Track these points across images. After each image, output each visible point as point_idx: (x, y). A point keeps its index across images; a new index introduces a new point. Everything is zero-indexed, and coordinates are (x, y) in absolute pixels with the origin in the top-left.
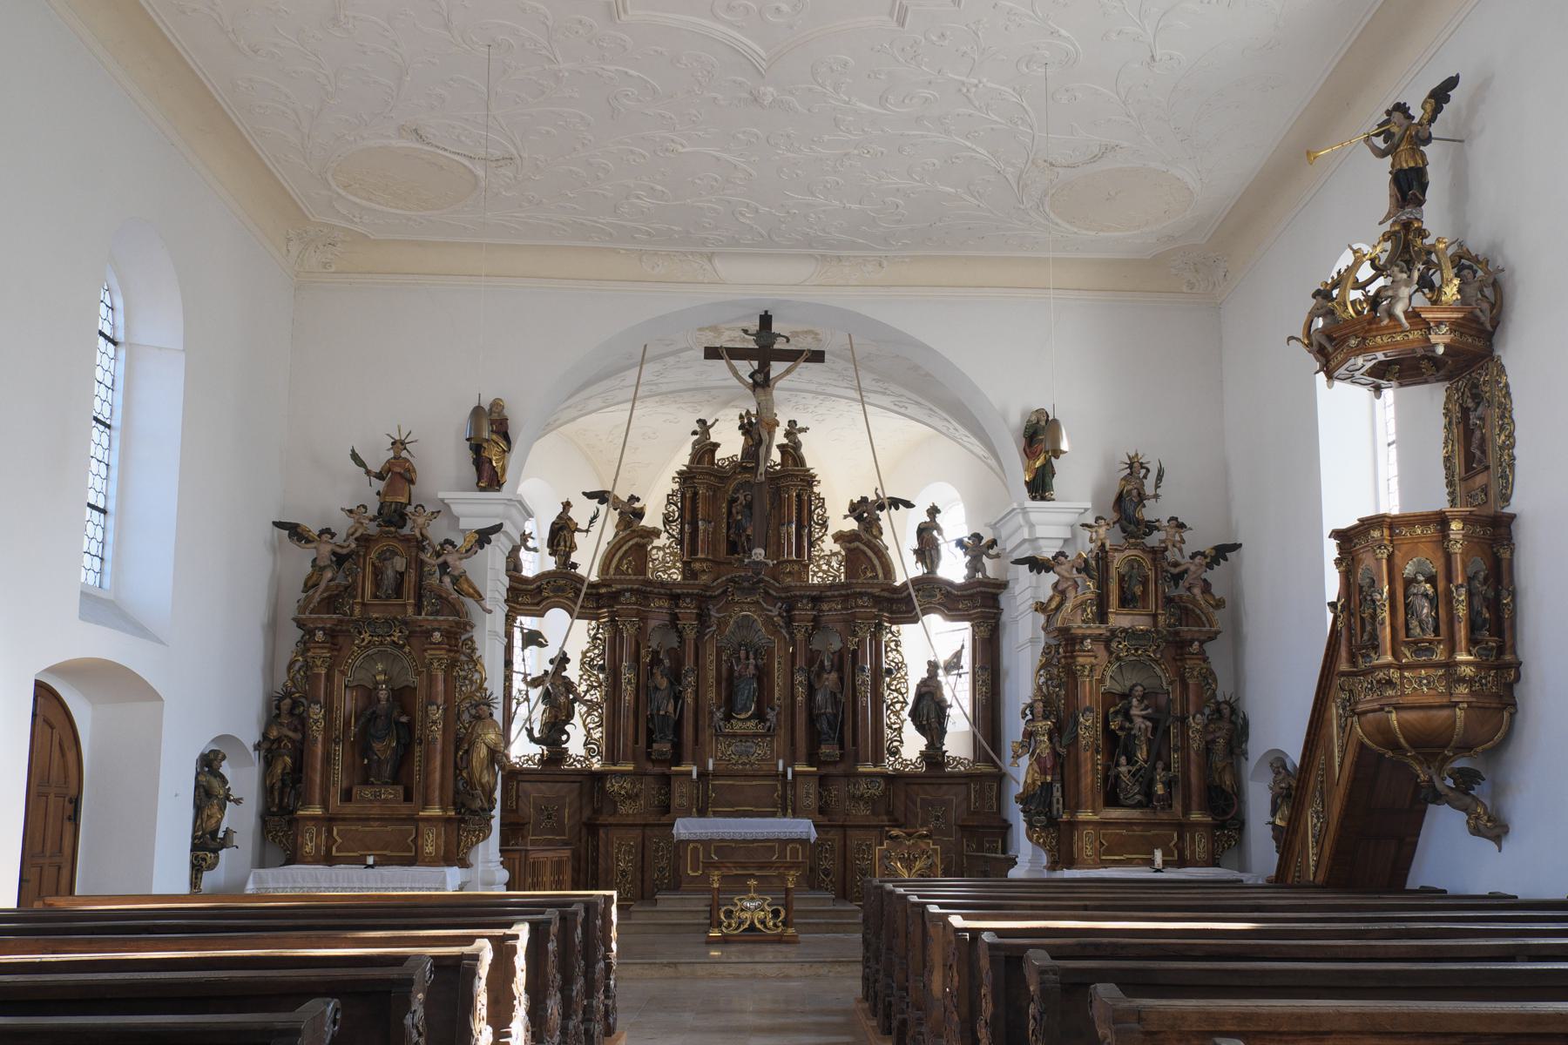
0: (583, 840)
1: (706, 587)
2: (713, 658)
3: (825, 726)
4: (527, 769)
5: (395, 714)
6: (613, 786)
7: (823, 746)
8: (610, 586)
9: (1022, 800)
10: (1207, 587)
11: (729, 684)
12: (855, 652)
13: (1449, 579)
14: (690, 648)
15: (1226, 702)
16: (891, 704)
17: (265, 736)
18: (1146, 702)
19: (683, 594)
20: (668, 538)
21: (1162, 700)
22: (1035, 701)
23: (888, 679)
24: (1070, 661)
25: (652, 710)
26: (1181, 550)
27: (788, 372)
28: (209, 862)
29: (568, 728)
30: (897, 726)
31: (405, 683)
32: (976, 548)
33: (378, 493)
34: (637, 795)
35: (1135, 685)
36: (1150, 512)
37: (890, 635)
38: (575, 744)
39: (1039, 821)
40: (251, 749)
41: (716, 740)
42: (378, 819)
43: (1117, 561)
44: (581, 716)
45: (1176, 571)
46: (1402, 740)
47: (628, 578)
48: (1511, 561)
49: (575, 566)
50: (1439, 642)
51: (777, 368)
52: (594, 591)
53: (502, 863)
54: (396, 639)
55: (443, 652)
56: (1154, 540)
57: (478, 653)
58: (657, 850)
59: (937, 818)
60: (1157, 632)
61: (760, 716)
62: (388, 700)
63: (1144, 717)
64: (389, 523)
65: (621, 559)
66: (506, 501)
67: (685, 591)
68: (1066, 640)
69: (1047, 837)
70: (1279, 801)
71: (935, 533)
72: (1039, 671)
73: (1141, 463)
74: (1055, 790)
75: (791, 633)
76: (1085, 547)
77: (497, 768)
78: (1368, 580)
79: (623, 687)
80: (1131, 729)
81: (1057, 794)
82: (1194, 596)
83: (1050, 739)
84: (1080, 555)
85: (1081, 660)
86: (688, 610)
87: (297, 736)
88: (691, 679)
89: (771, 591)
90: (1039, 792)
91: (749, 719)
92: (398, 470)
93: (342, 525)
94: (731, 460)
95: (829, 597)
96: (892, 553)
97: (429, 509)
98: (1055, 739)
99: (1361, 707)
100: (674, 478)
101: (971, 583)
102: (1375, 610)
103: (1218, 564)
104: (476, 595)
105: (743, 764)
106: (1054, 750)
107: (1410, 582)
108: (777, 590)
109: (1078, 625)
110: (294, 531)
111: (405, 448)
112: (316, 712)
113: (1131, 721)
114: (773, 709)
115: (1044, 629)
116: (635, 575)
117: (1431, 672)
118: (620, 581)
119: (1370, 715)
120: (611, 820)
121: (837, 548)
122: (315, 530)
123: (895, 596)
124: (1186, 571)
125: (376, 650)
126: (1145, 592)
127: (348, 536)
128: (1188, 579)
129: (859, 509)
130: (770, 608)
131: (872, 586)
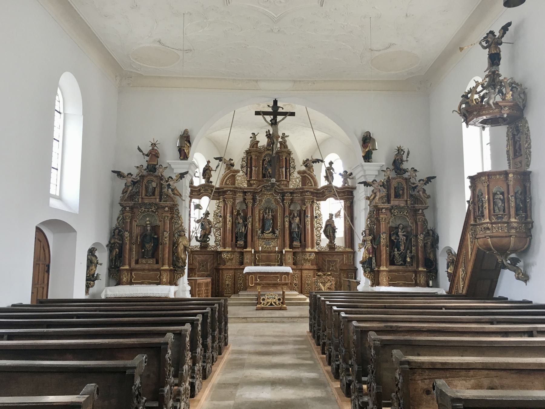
0: (214, 274)
1: (255, 189)
2: (257, 212)
3: (295, 235)
4: (195, 250)
5: (153, 235)
6: (224, 256)
7: (294, 242)
8: (223, 189)
10: (424, 191)
11: (263, 221)
12: (305, 211)
13: (508, 194)
14: (250, 210)
15: (431, 230)
16: (317, 228)
17: (110, 242)
18: (404, 230)
19: (248, 191)
20: (242, 173)
21: (409, 229)
22: (366, 230)
23: (315, 220)
24: (378, 216)
25: (237, 230)
26: (415, 179)
27: (283, 119)
28: (91, 285)
29: (209, 236)
30: (319, 235)
31: (156, 224)
32: (347, 175)
33: (147, 161)
34: (232, 259)
35: (400, 224)
36: (405, 166)
37: (316, 205)
38: (212, 242)
39: (367, 270)
40: (105, 246)
41: (259, 240)
42: (147, 270)
43: (394, 184)
44: (214, 232)
45: (413, 186)
46: (492, 248)
47: (229, 186)
48: (530, 187)
49: (211, 182)
50: (505, 215)
51: (279, 118)
52: (218, 191)
53: (188, 284)
54: (153, 210)
55: (169, 214)
56: (406, 175)
58: (239, 277)
59: (333, 266)
60: (408, 207)
61: (273, 232)
62: (150, 230)
63: (403, 235)
64: (150, 171)
65: (227, 180)
67: (248, 190)
68: (376, 209)
69: (370, 275)
70: (449, 264)
71: (332, 170)
73: (402, 150)
74: (373, 259)
75: (283, 204)
76: (382, 178)
77: (187, 253)
78: (480, 193)
79: (228, 223)
80: (399, 239)
81: (374, 261)
82: (420, 194)
83: (371, 243)
84: (381, 181)
85: (381, 216)
86: (249, 197)
87: (121, 242)
88: (250, 220)
89: (277, 190)
91: (269, 233)
92: (153, 153)
93: (135, 172)
94: (263, 146)
95: (296, 192)
96: (317, 178)
97: (164, 166)
98: (373, 242)
99: (477, 237)
100: (244, 153)
101: (343, 188)
102: (483, 203)
103: (428, 183)
105: (268, 248)
106: (372, 246)
107: (495, 194)
108: (279, 190)
109: (381, 205)
110: (119, 174)
111: (156, 146)
112: (127, 234)
113: (399, 236)
114: (277, 230)
115: (369, 205)
116: (231, 185)
117: (502, 225)
118: (227, 187)
119: (481, 239)
120: (223, 267)
121: (299, 176)
122: (126, 174)
123: (318, 192)
124: (417, 186)
126: (403, 193)
127: (137, 176)
128: (418, 188)
129: (306, 163)
130: (276, 196)
131: (311, 188)
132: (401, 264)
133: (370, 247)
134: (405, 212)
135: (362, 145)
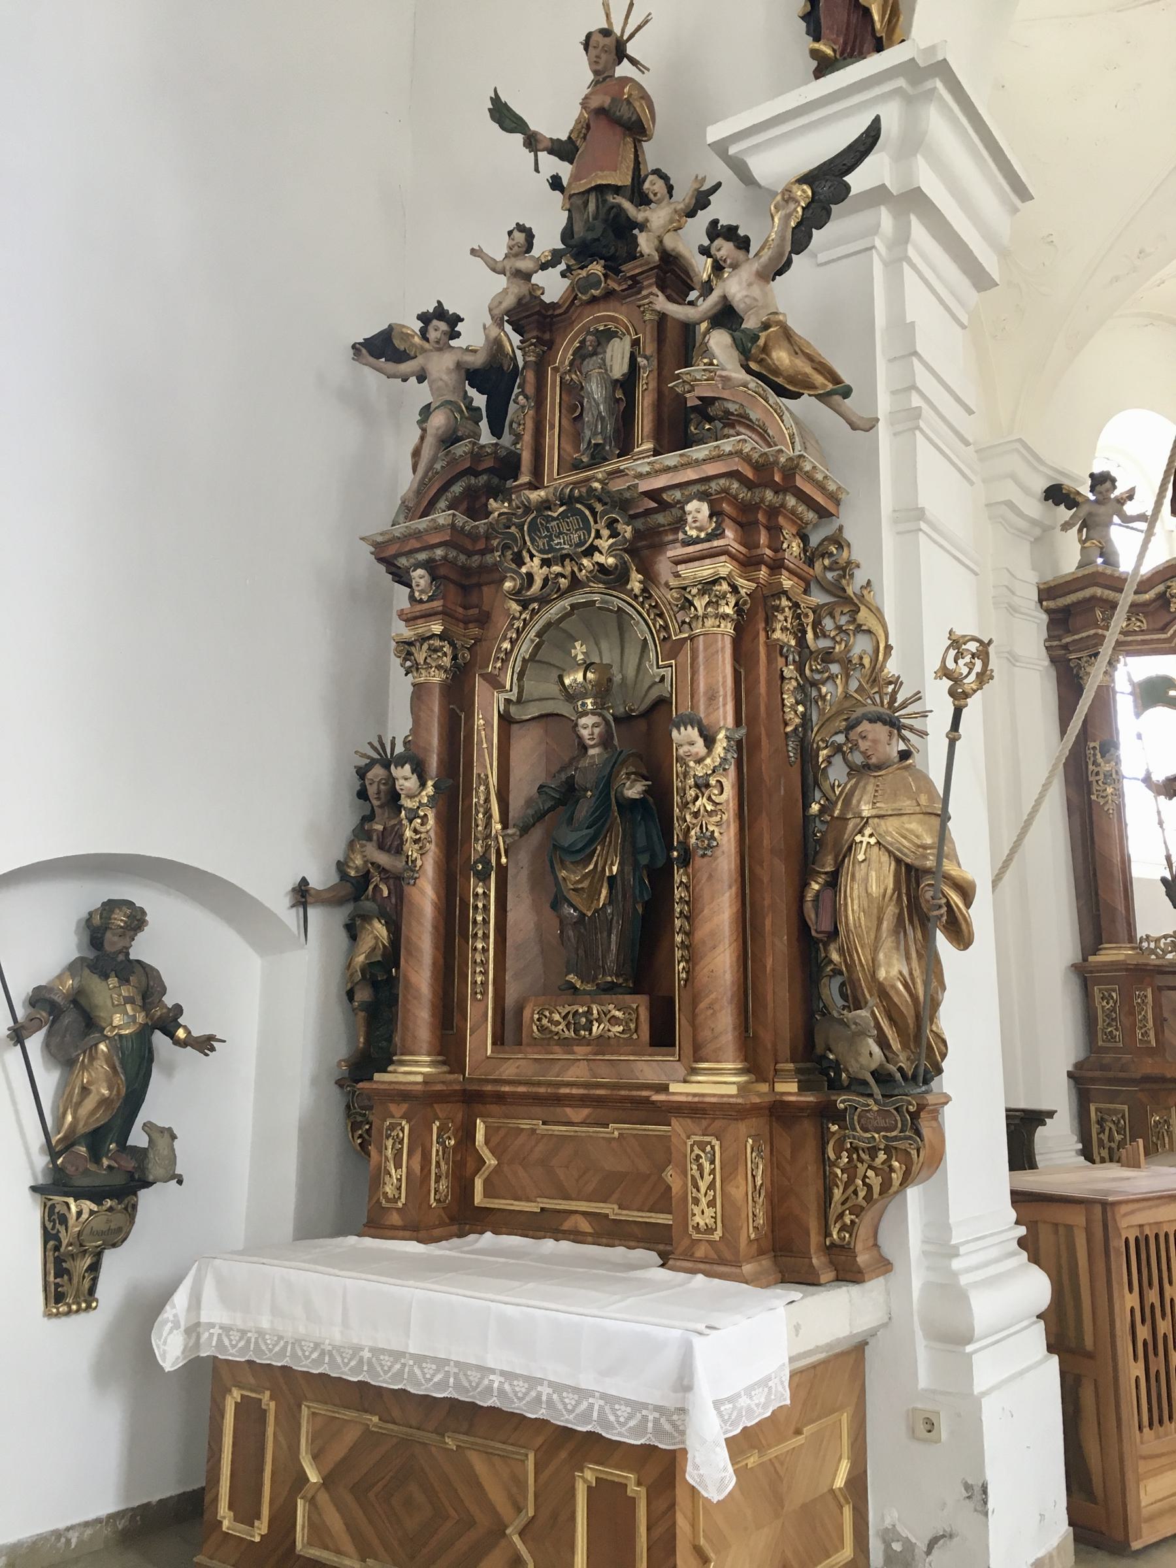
31: (654, 694)
42: (583, 1101)
57: (860, 577)
62: (605, 741)
66: (901, 82)
104: (819, 379)
125: (565, 603)
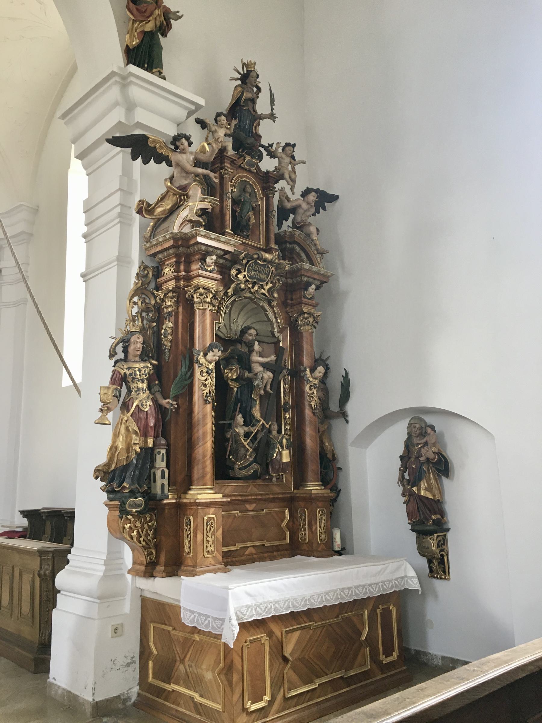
9: (105, 473)
39: (135, 505)
69: (142, 528)
72: (133, 297)
74: (159, 458)
81: (161, 464)
83: (149, 387)
90: (135, 462)
103: (319, 213)
113: (250, 370)
124: (294, 210)
132: (256, 472)
133: (148, 406)
134: (267, 288)
135: (128, 7)
